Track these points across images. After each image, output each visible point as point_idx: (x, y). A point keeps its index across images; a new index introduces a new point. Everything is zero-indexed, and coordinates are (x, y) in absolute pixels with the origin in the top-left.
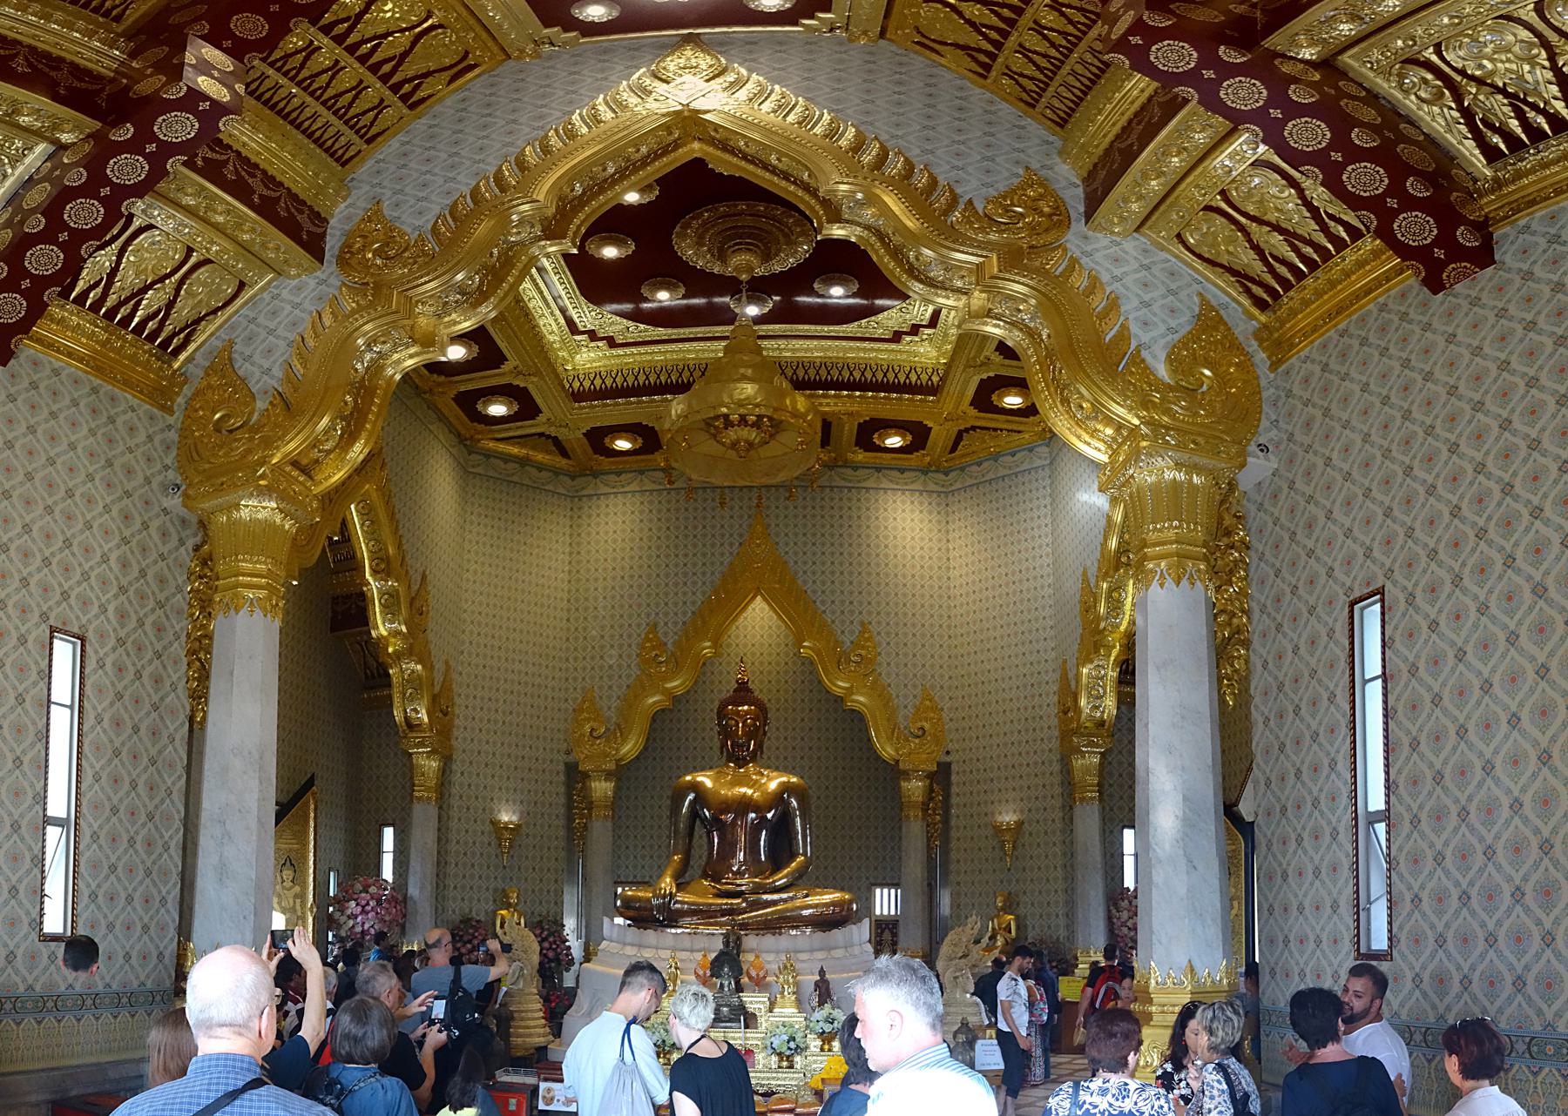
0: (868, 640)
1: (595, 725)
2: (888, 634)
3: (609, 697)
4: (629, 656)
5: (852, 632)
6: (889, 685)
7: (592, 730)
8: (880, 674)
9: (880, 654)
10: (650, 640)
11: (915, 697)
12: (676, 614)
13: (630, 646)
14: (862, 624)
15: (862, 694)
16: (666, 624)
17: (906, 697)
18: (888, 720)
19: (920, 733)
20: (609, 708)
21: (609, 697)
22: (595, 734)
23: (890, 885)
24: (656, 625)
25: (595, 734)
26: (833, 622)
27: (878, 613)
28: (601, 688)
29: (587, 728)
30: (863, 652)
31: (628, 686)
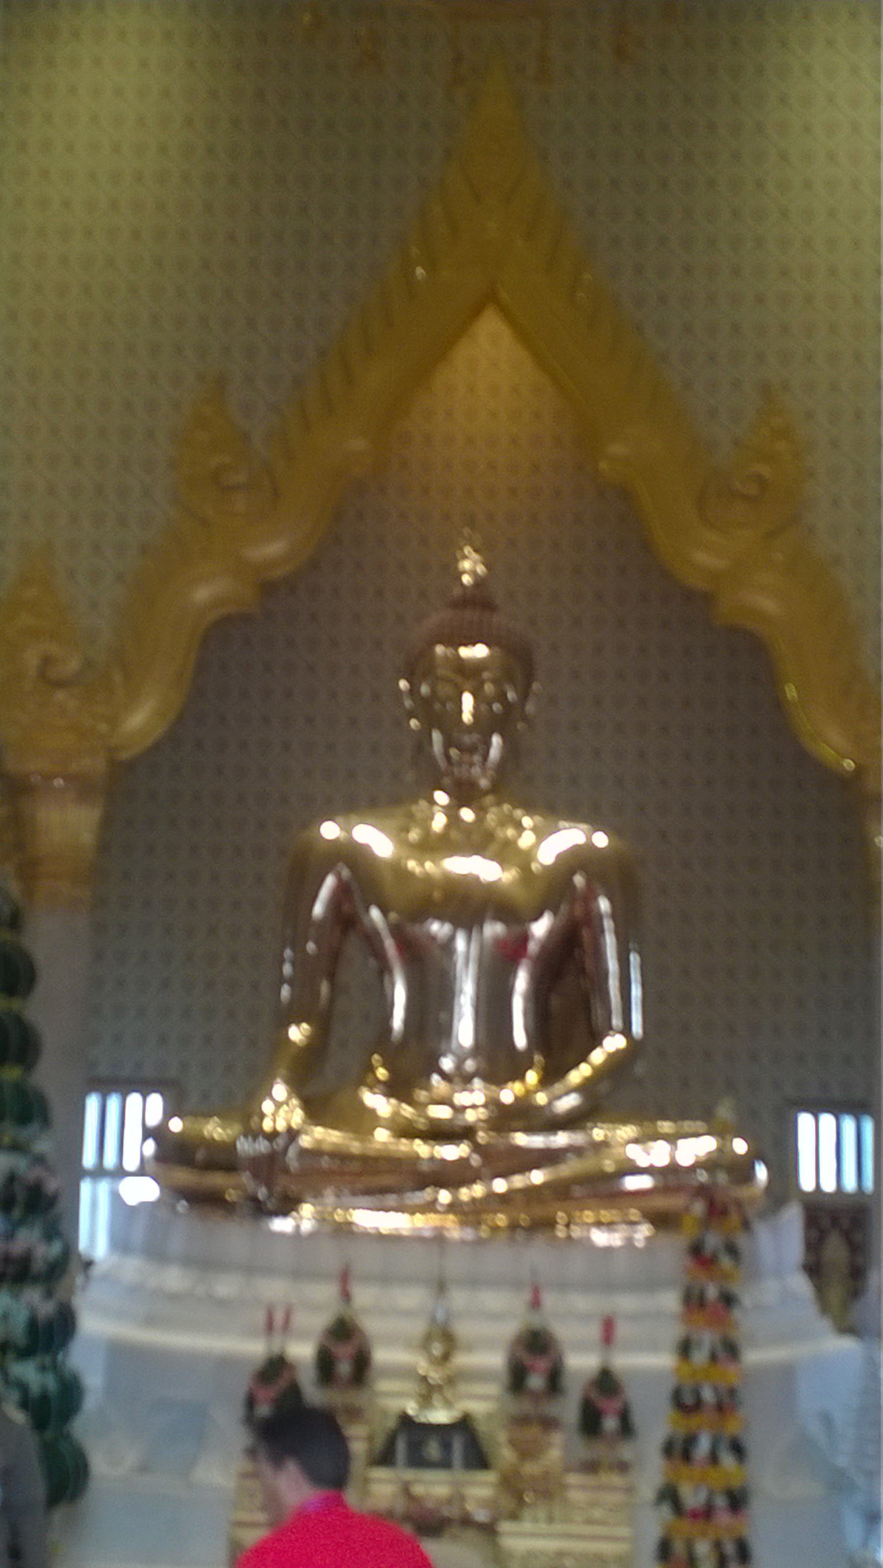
7: (47, 661)
23: (838, 1109)
29: (31, 658)
30: (765, 470)
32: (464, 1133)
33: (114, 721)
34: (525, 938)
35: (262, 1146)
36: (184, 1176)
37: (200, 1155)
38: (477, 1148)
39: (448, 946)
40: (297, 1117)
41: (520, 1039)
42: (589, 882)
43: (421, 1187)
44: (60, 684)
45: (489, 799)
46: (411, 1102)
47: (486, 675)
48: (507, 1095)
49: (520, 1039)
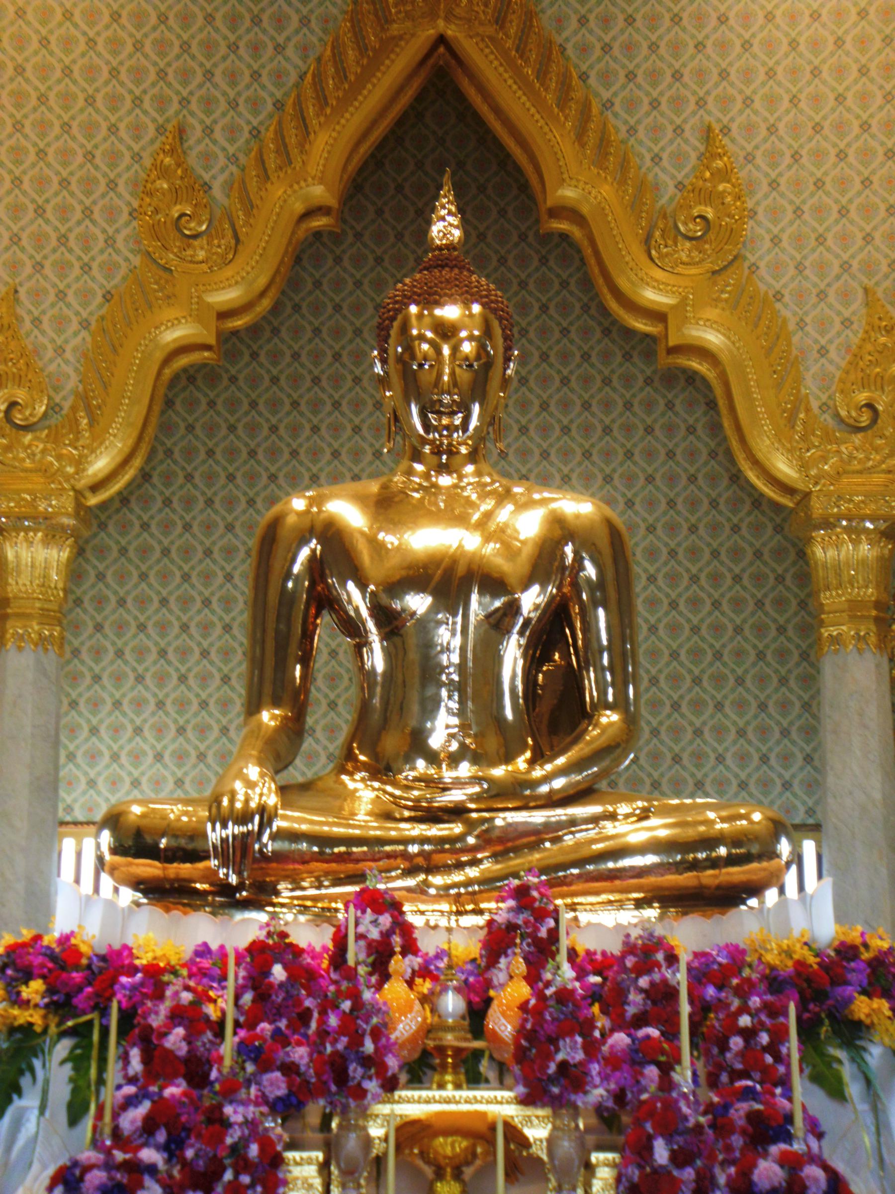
0: (724, 175)
1: (21, 395)
2: (773, 157)
3: (60, 323)
4: (111, 214)
5: (679, 158)
6: (778, 296)
7: (13, 405)
8: (753, 268)
9: (753, 214)
10: (164, 173)
11: (847, 323)
12: (233, 105)
13: (112, 185)
14: (708, 134)
15: (710, 324)
16: (208, 131)
17: (823, 325)
18: (779, 386)
19: (865, 419)
20: (60, 351)
21: (60, 323)
22: (18, 418)
24: (181, 132)
25: (18, 418)
26: (632, 131)
27: (748, 102)
28: (37, 294)
30: (710, 213)
31: (108, 297)
32: (457, 812)
33: (80, 463)
34: (513, 608)
35: (233, 829)
36: (148, 868)
37: (163, 843)
38: (471, 825)
39: (425, 625)
40: (272, 800)
41: (509, 714)
42: (576, 553)
43: (410, 872)
44: (26, 428)
45: (470, 469)
46: (395, 784)
47: (464, 334)
48: (499, 772)
49: (509, 714)
